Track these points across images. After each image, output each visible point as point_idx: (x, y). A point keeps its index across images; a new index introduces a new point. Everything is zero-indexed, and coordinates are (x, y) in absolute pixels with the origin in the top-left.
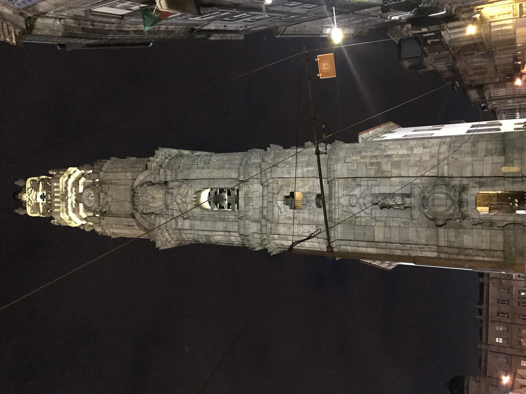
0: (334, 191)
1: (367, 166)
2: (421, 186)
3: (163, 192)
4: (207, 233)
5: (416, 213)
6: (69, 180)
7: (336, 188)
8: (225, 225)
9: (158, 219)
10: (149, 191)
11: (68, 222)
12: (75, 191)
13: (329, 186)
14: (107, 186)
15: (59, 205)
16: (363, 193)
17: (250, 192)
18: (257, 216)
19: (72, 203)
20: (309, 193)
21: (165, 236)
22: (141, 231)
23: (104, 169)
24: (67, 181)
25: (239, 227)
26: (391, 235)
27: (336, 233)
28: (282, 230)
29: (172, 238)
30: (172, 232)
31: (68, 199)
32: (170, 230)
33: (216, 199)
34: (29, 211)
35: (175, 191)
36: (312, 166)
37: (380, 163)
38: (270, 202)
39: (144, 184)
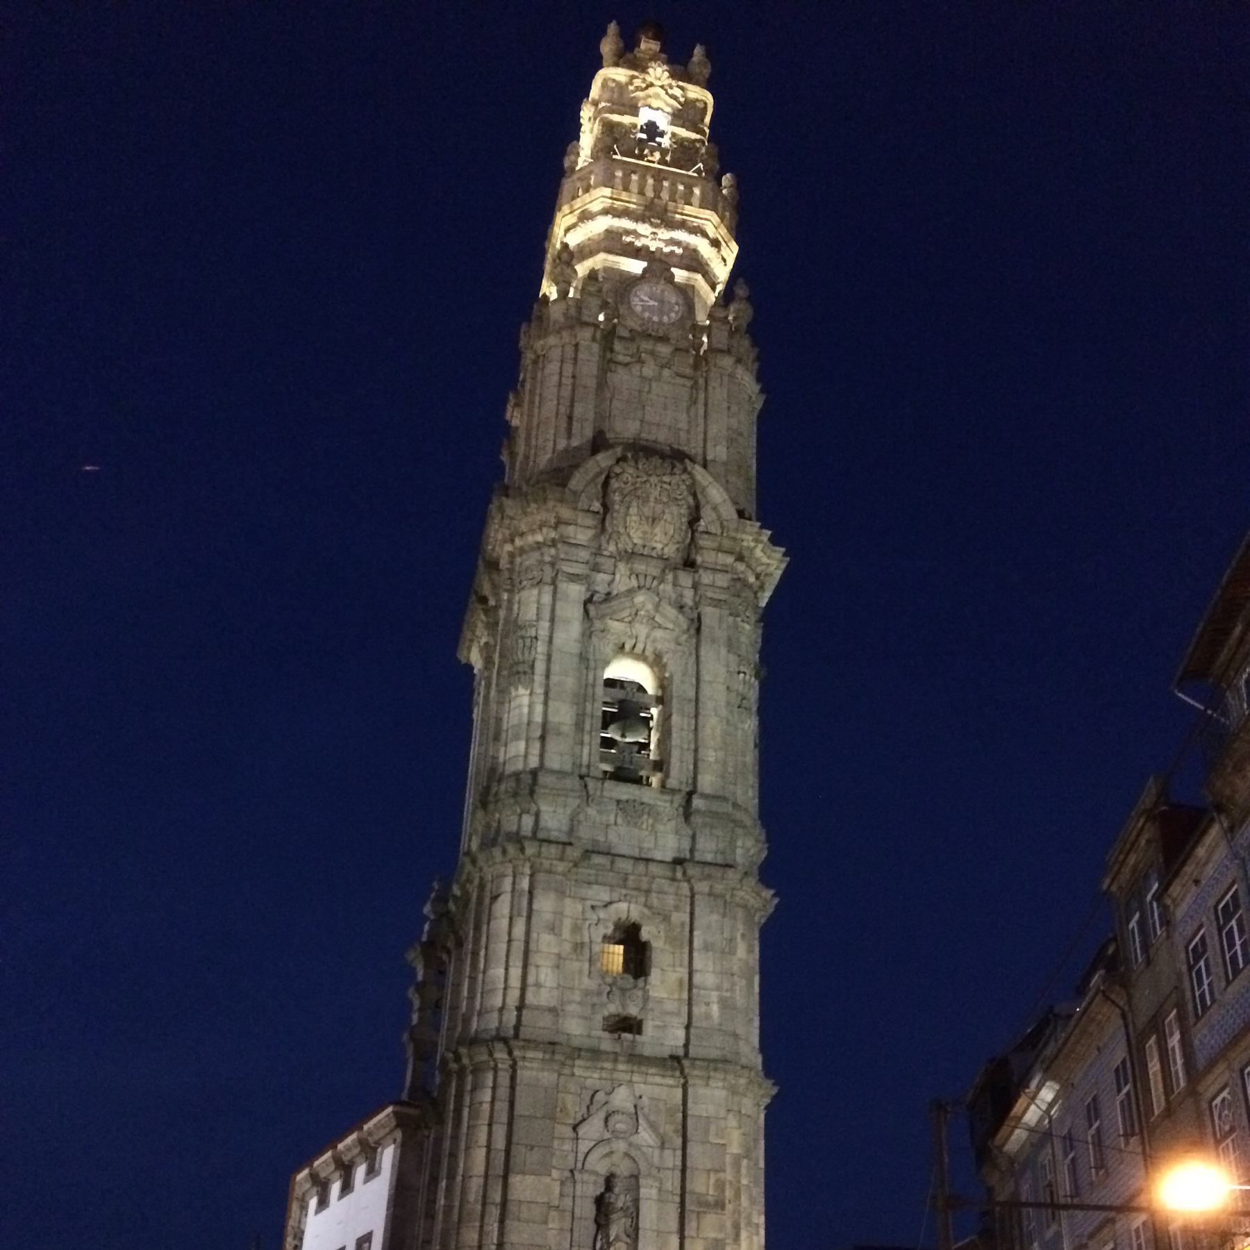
0: (652, 1071)
1: (717, 1171)
3: (670, 551)
4: (540, 667)
6: (706, 241)
7: (658, 1079)
9: (590, 521)
10: (675, 509)
11: (578, 203)
12: (672, 252)
13: (665, 1059)
14: (688, 371)
15: (634, 187)
16: (644, 1154)
17: (656, 820)
18: (585, 833)
19: (638, 235)
20: (646, 999)
21: (533, 532)
22: (548, 456)
23: (740, 371)
24: (705, 234)
25: (561, 774)
26: (527, 1221)
27: (535, 1065)
28: (545, 904)
29: (522, 551)
30: (547, 559)
31: (652, 224)
32: (553, 551)
33: (625, 707)
34: (612, 73)
35: (667, 588)
36: (722, 1015)
37: (723, 1208)
38: (626, 880)
39: (695, 495)
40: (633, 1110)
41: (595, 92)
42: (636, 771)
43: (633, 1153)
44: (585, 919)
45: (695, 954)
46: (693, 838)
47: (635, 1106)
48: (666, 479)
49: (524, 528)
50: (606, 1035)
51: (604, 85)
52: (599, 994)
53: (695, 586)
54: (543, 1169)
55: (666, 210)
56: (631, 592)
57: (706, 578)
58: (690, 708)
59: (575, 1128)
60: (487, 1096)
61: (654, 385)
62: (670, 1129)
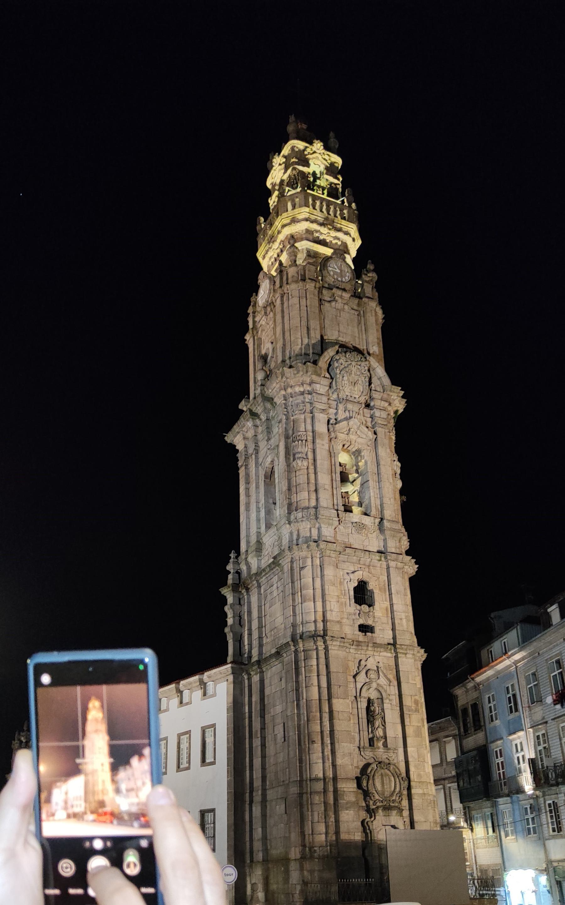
2: (395, 761)
5: (368, 754)
8: (327, 487)
12: (336, 243)
27: (336, 648)
28: (329, 572)
30: (307, 400)
38: (360, 560)
40: (376, 668)
41: (286, 150)
42: (351, 507)
43: (380, 689)
44: (344, 579)
45: (393, 596)
46: (385, 540)
47: (377, 667)
48: (359, 363)
49: (292, 383)
50: (360, 633)
51: (293, 148)
52: (355, 614)
53: (372, 417)
54: (346, 697)
55: (333, 222)
56: (346, 419)
57: (377, 413)
58: (376, 477)
59: (354, 677)
60: (314, 662)
61: (342, 312)
62: (392, 676)
